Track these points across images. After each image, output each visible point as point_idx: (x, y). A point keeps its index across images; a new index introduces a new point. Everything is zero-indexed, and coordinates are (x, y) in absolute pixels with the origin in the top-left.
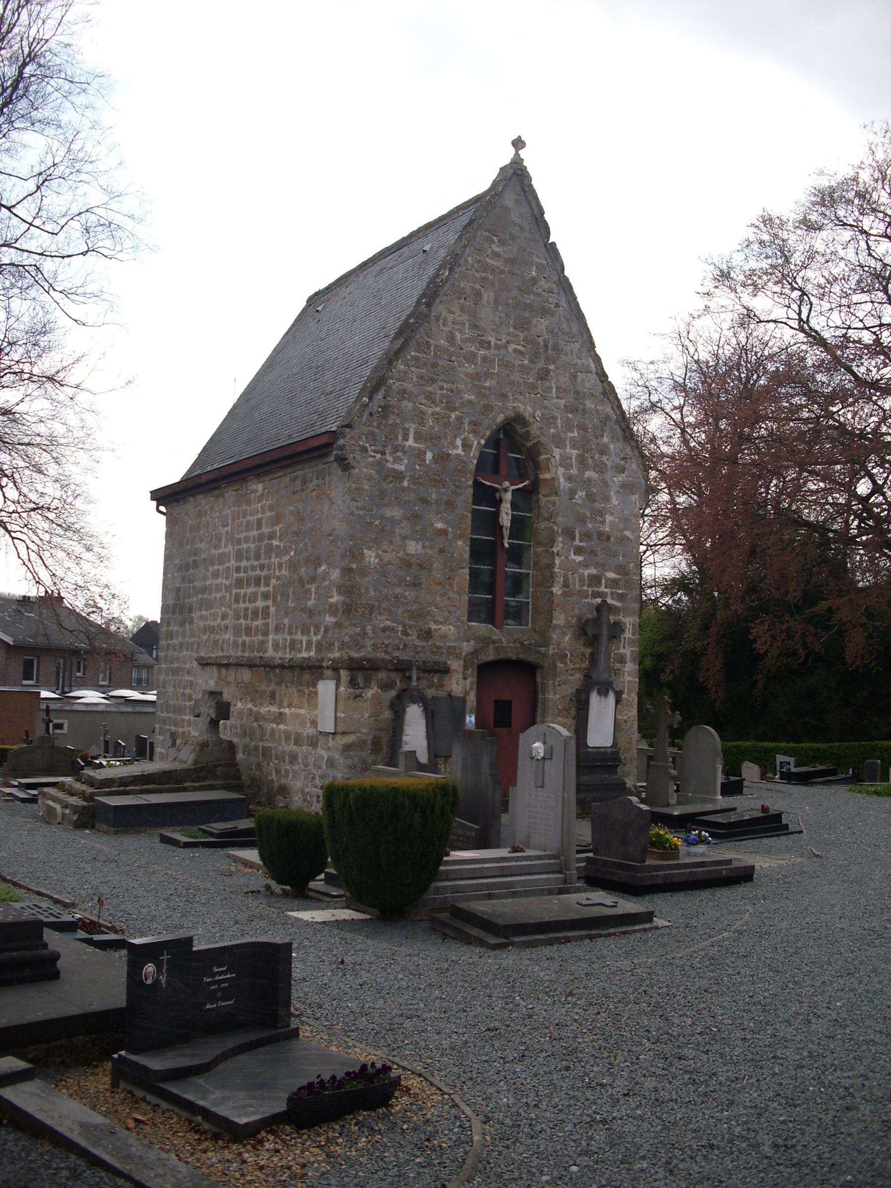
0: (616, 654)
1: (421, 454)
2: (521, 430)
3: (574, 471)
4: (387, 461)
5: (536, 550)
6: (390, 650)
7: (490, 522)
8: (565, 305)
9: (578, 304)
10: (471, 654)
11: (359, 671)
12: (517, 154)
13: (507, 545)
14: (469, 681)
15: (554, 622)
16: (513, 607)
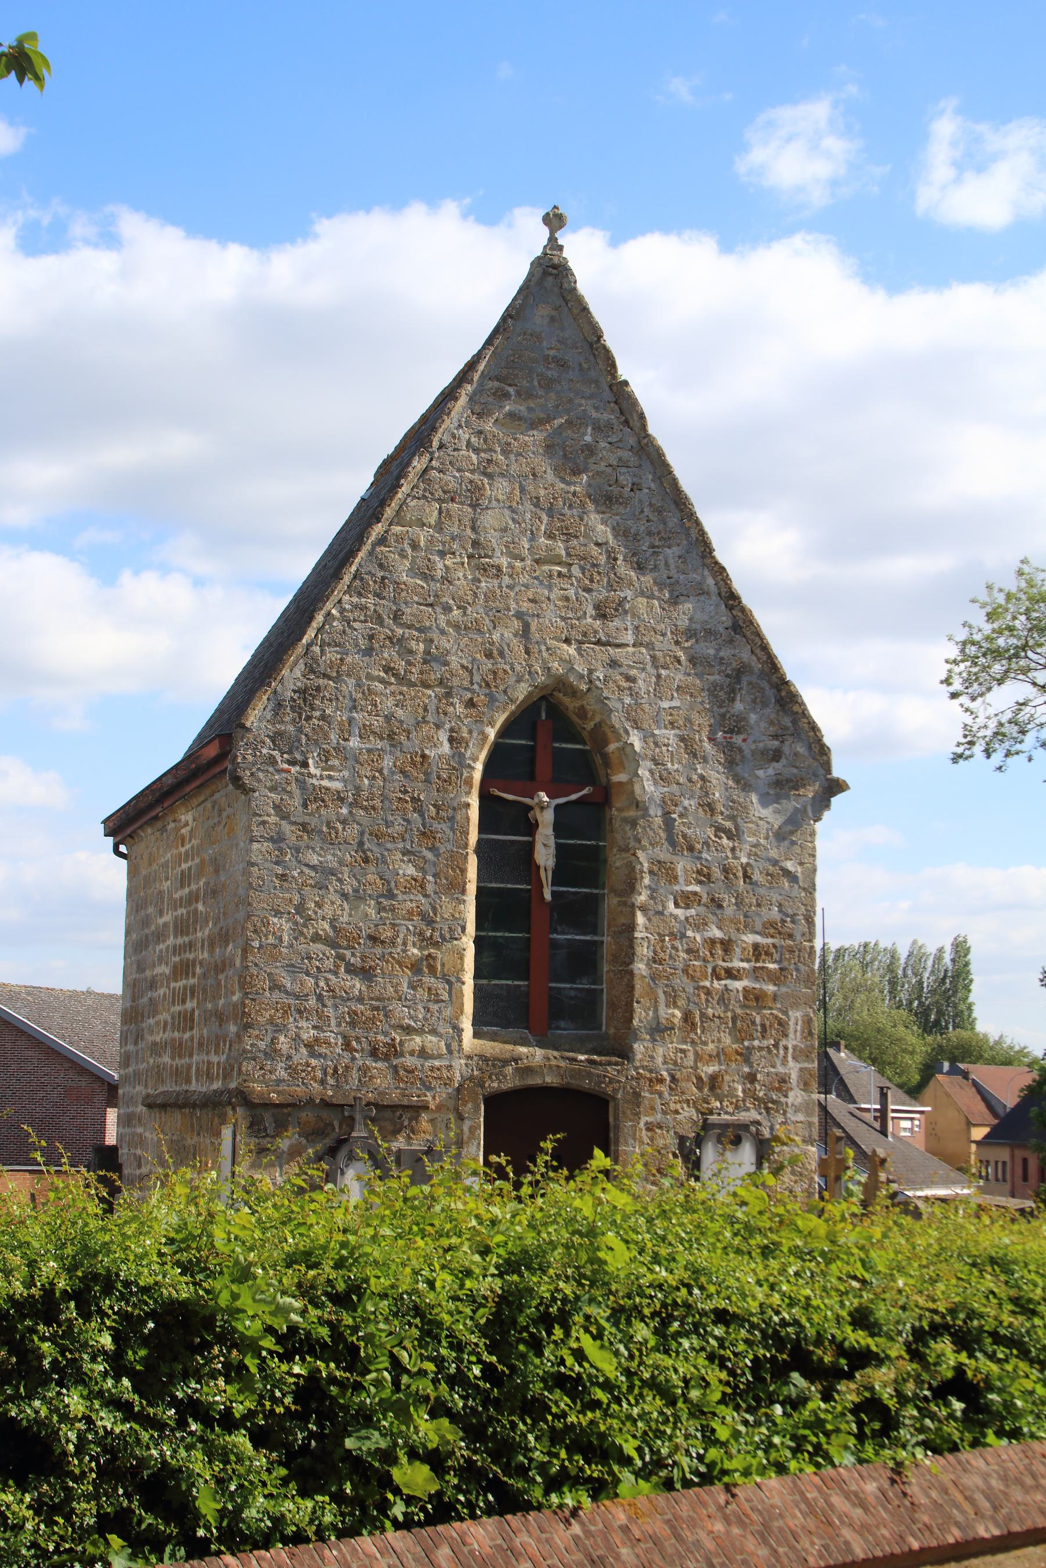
4: (310, 775)
8: (653, 486)
9: (674, 482)
12: (552, 240)
13: (548, 896)
16: (571, 998)
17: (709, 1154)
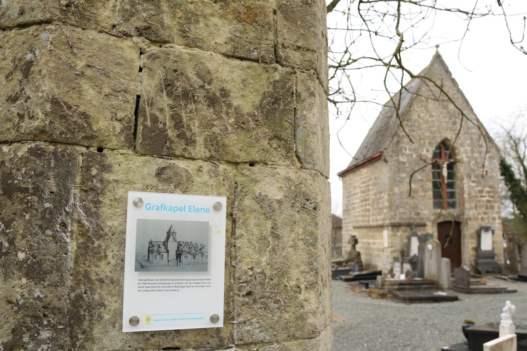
1: (411, 155)
2: (448, 143)
3: (469, 155)
5: (458, 183)
7: (440, 175)
11: (395, 226)
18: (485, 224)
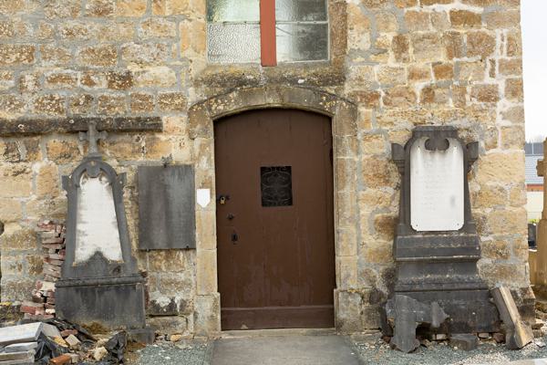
0: (476, 87)
6: (64, 106)
10: (200, 103)
14: (198, 141)
15: (350, 44)
17: (420, 160)
18: (436, 116)
